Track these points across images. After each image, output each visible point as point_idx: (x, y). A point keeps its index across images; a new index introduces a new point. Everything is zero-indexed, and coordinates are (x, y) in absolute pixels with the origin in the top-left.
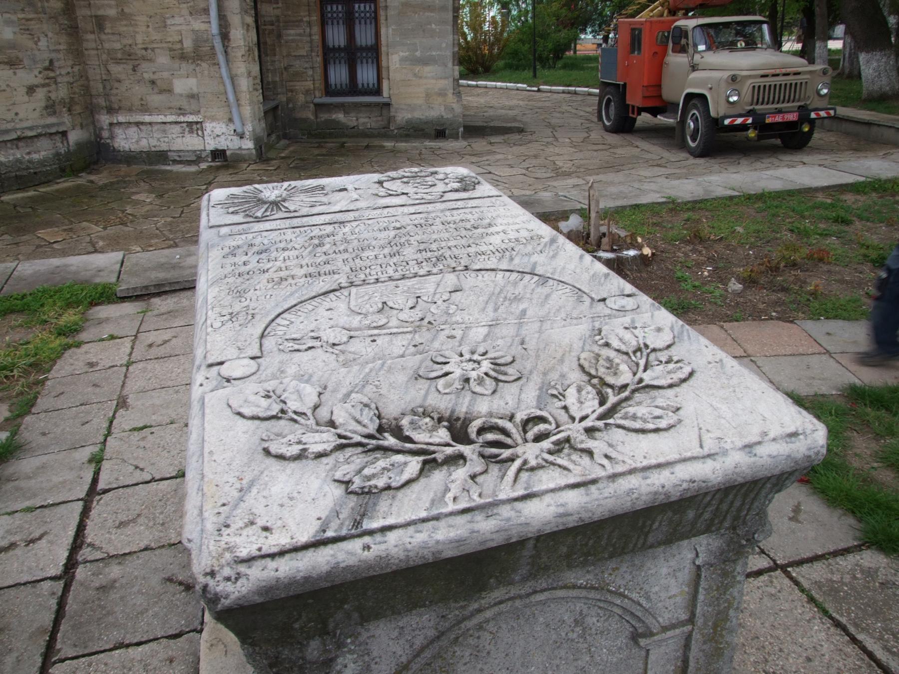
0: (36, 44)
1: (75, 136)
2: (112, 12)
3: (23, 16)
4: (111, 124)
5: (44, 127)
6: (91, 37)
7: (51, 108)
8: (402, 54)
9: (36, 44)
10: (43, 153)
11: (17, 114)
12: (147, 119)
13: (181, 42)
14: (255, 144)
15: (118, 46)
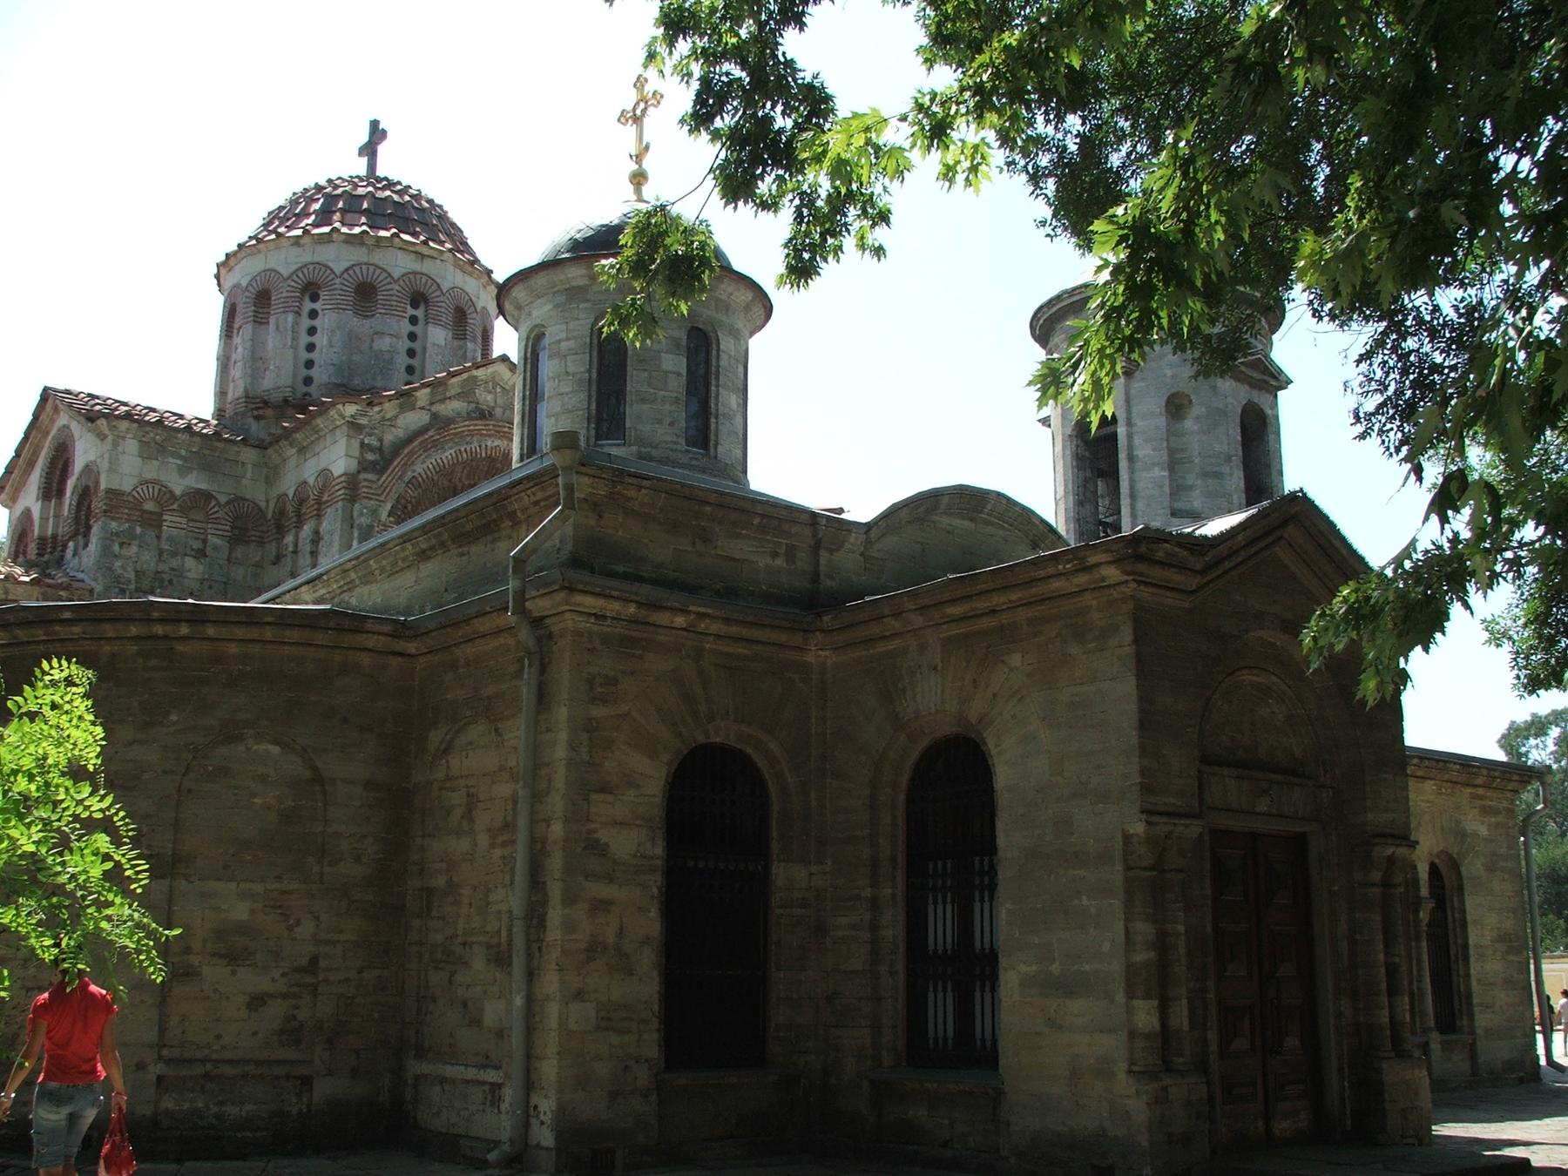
0: (290, 929)
1: (323, 1089)
2: (440, 881)
3: (277, 886)
4: (417, 1078)
5: (259, 1063)
6: (416, 922)
7: (291, 1033)
8: (1024, 968)
9: (290, 929)
10: (249, 1107)
11: (218, 1037)
12: (449, 1071)
13: (499, 931)
14: (559, 1135)
15: (439, 938)
